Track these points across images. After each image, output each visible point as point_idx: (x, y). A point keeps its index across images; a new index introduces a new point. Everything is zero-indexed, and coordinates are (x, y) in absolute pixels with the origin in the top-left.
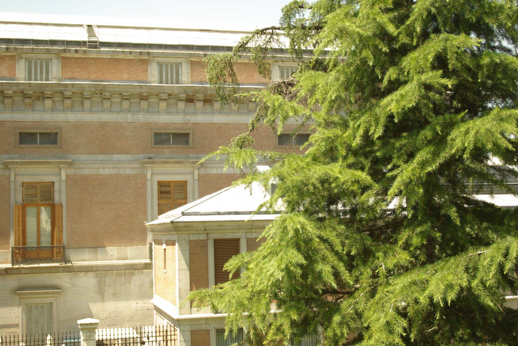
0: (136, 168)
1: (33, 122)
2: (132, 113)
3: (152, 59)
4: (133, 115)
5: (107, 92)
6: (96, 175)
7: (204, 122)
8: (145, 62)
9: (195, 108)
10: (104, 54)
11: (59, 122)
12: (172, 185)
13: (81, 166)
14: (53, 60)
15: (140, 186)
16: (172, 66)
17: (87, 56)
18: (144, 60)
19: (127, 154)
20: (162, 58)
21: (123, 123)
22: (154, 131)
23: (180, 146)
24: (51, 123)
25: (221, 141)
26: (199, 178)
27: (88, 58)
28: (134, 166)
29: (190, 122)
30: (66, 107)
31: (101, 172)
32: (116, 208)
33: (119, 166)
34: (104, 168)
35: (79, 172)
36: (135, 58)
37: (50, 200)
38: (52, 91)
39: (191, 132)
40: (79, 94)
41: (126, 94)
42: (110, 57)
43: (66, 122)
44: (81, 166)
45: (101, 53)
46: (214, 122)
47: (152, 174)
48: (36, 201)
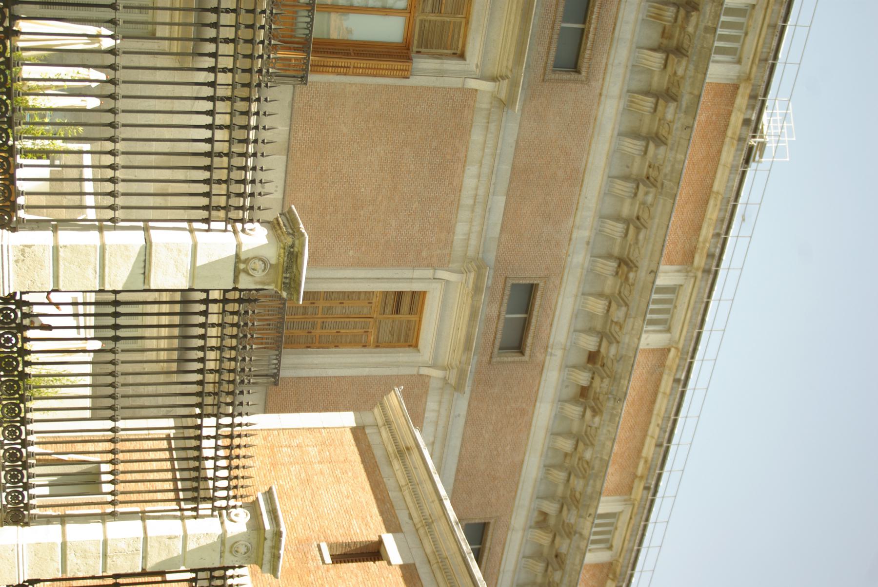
0: (467, 247)
1: (616, 18)
2: (591, 241)
3: (691, 274)
4: (588, 243)
5: (655, 197)
6: (466, 156)
7: (542, 383)
8: (688, 258)
9: (574, 367)
10: (728, 181)
11: (604, 79)
12: (413, 318)
13: (493, 127)
14: (737, 67)
15: (424, 254)
16: (667, 311)
17: (727, 140)
18: (693, 257)
19: (502, 227)
20: (689, 295)
21: (572, 219)
22: (541, 284)
23: (499, 336)
24: (604, 61)
25: (494, 418)
26: (421, 375)
27: (723, 142)
28: (473, 242)
29: (548, 358)
30: (634, 97)
31: (472, 170)
32: (380, 198)
33: (479, 210)
34: (479, 176)
35: (479, 120)
36: (701, 239)
37: (420, 45)
38: (683, 78)
39: (526, 358)
40: (658, 128)
41: (641, 237)
42: (715, 188)
43: (600, 94)
44: (493, 127)
45: (730, 173)
46: (538, 404)
47: (447, 282)
48: (423, 11)
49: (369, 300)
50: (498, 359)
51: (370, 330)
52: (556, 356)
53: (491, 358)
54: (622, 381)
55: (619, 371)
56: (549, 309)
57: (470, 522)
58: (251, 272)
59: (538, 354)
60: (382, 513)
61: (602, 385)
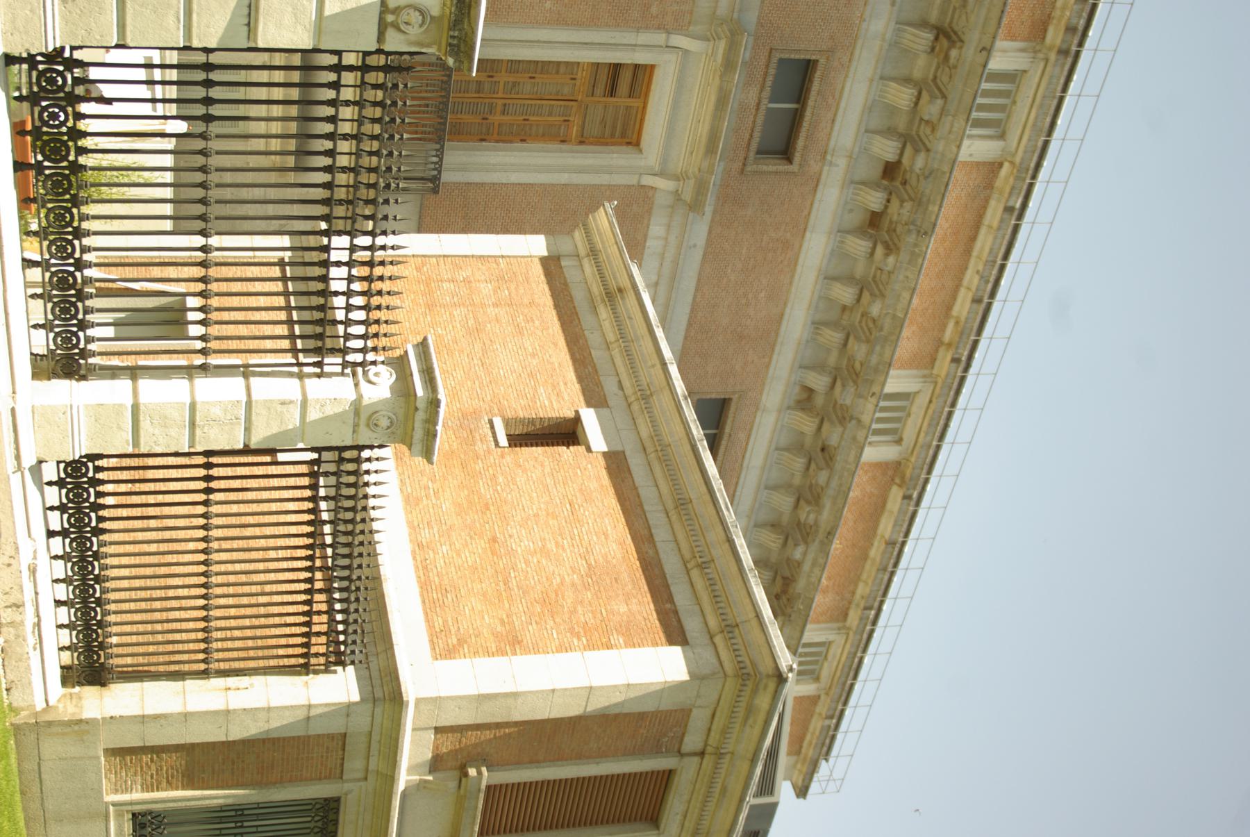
7: (816, 205)
9: (863, 183)
12: (635, 103)
22: (822, 61)
23: (757, 134)
25: (744, 251)
29: (826, 168)
39: (794, 168)
46: (808, 234)
47: (686, 52)
49: (572, 74)
50: (755, 166)
51: (571, 119)
52: (837, 166)
53: (744, 165)
54: (930, 208)
55: (928, 191)
56: (831, 97)
57: (704, 397)
58: (403, 27)
59: (812, 162)
60: (580, 379)
61: (901, 211)
